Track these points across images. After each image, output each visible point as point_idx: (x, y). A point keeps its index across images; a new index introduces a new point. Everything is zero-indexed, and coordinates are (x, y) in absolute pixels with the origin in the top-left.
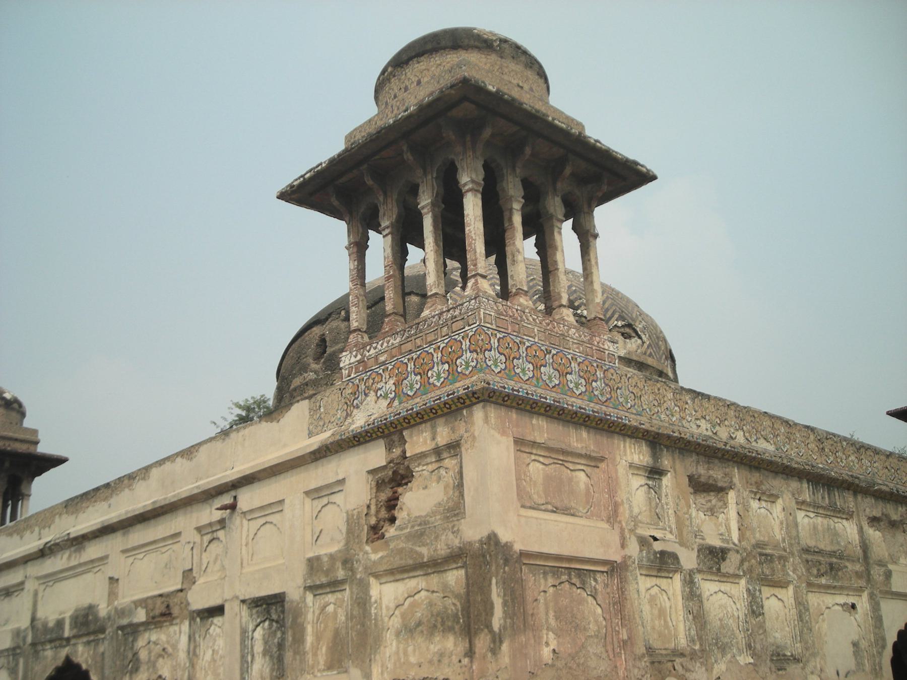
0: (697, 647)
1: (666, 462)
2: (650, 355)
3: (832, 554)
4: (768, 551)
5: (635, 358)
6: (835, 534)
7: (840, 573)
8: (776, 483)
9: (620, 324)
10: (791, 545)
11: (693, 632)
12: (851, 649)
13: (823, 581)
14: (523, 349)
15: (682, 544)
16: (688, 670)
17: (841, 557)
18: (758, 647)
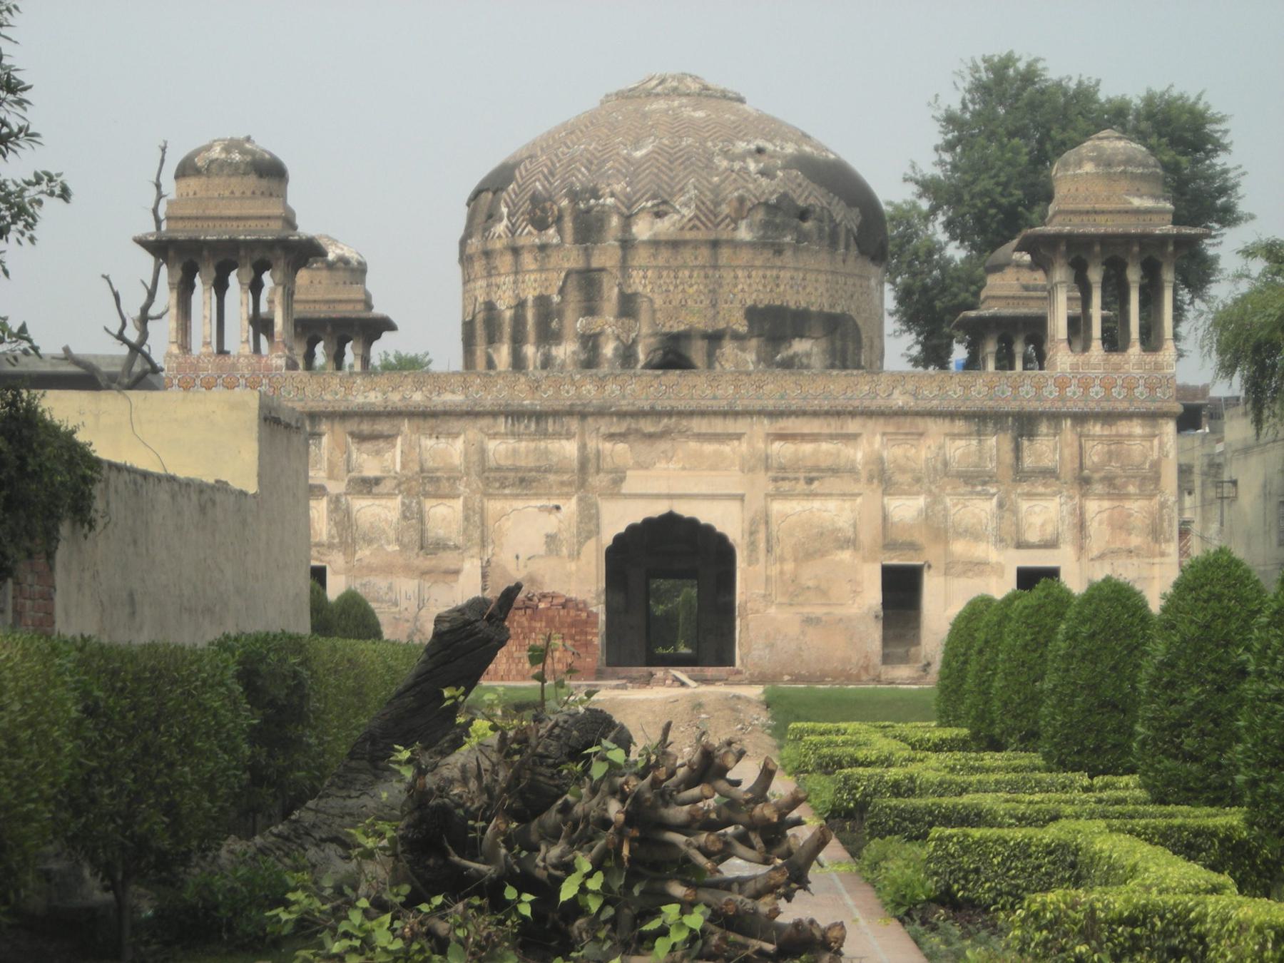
0: (336, 540)
1: (324, 427)
2: (694, 227)
3: (538, 469)
4: (439, 474)
5: (663, 238)
6: (546, 452)
7: (534, 484)
8: (455, 425)
9: (649, 204)
10: (467, 468)
11: (334, 531)
12: (544, 539)
13: (507, 491)
14: (198, 382)
15: (331, 476)
16: (323, 554)
17: (545, 471)
18: (406, 540)
